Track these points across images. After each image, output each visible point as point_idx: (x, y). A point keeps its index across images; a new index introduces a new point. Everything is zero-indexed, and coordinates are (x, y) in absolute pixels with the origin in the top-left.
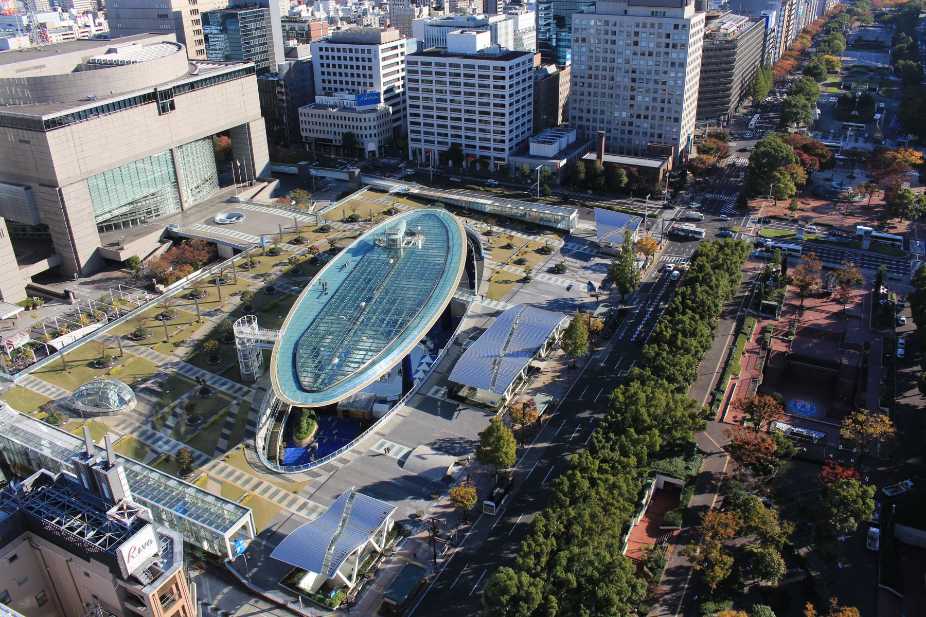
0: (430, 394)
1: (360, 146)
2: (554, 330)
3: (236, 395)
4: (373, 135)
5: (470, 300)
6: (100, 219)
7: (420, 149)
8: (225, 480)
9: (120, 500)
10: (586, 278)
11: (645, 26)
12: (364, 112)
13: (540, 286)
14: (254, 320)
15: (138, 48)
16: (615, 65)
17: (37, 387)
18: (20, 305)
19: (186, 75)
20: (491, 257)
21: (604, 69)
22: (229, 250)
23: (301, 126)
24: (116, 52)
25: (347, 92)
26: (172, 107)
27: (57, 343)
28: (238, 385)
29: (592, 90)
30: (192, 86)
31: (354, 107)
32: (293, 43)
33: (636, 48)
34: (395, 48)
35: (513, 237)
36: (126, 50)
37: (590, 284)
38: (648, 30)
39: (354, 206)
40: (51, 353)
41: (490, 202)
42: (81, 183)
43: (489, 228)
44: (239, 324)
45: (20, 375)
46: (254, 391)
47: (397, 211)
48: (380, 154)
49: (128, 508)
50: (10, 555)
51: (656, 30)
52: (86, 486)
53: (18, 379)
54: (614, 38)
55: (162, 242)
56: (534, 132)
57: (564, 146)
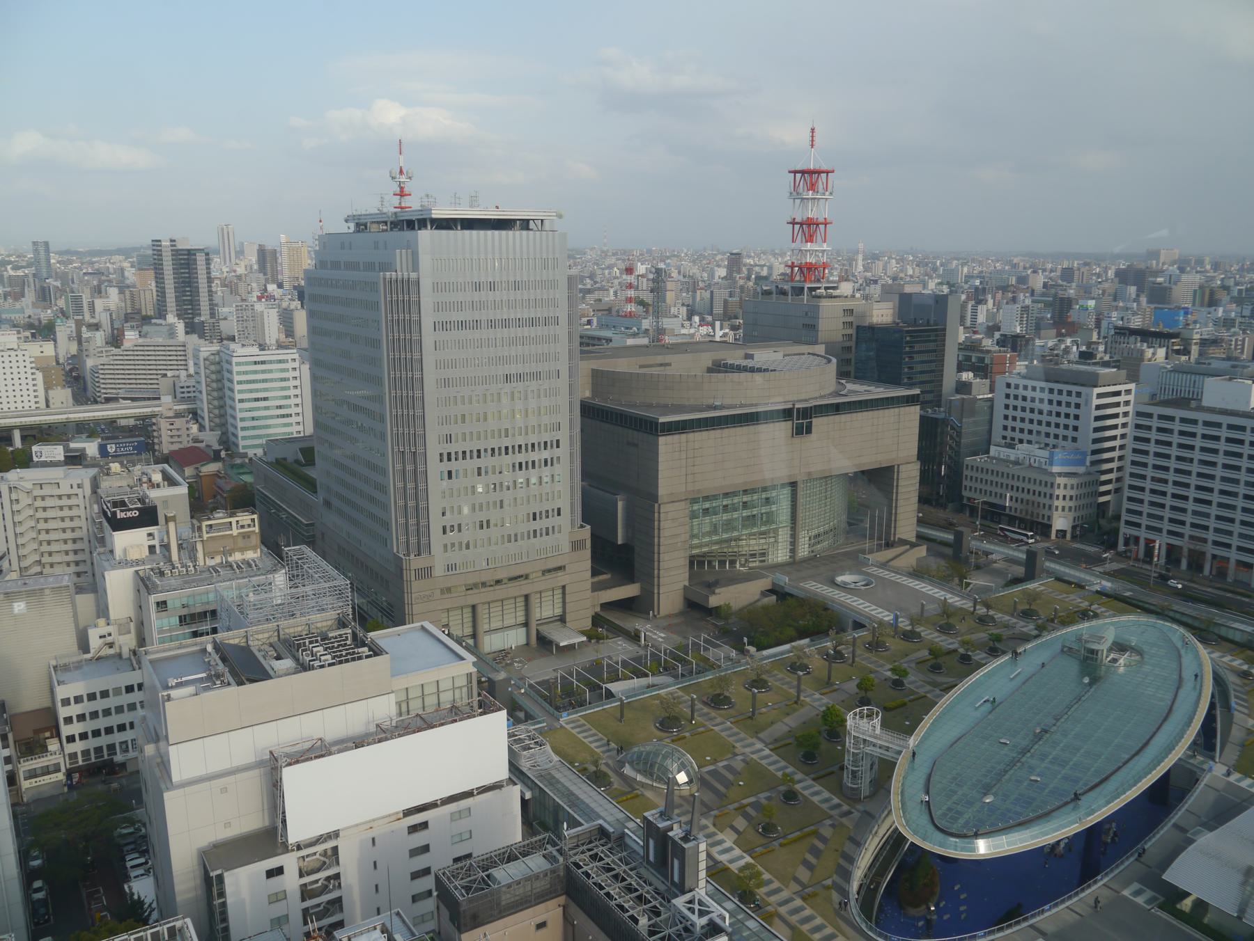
0: (1126, 893)
1: (1045, 521)
3: (833, 813)
4: (1067, 509)
5: (1206, 767)
6: (695, 552)
7: (1137, 539)
8: (798, 925)
9: (691, 891)
12: (1060, 474)
14: (877, 716)
15: (779, 356)
17: (585, 734)
18: (583, 633)
19: (830, 394)
20: (1246, 711)
22: (850, 624)
23: (965, 483)
24: (753, 359)
25: (1037, 446)
26: (809, 431)
27: (614, 687)
28: (836, 801)
30: (837, 409)
31: (1044, 467)
32: (967, 376)
34: (1118, 394)
36: (763, 356)
39: (1033, 597)
40: (607, 698)
42: (683, 502)
44: (855, 714)
45: (568, 715)
46: (856, 815)
47: (1096, 616)
48: (1074, 537)
49: (701, 903)
50: (539, 920)
52: (652, 858)
53: (565, 718)
55: (765, 593)
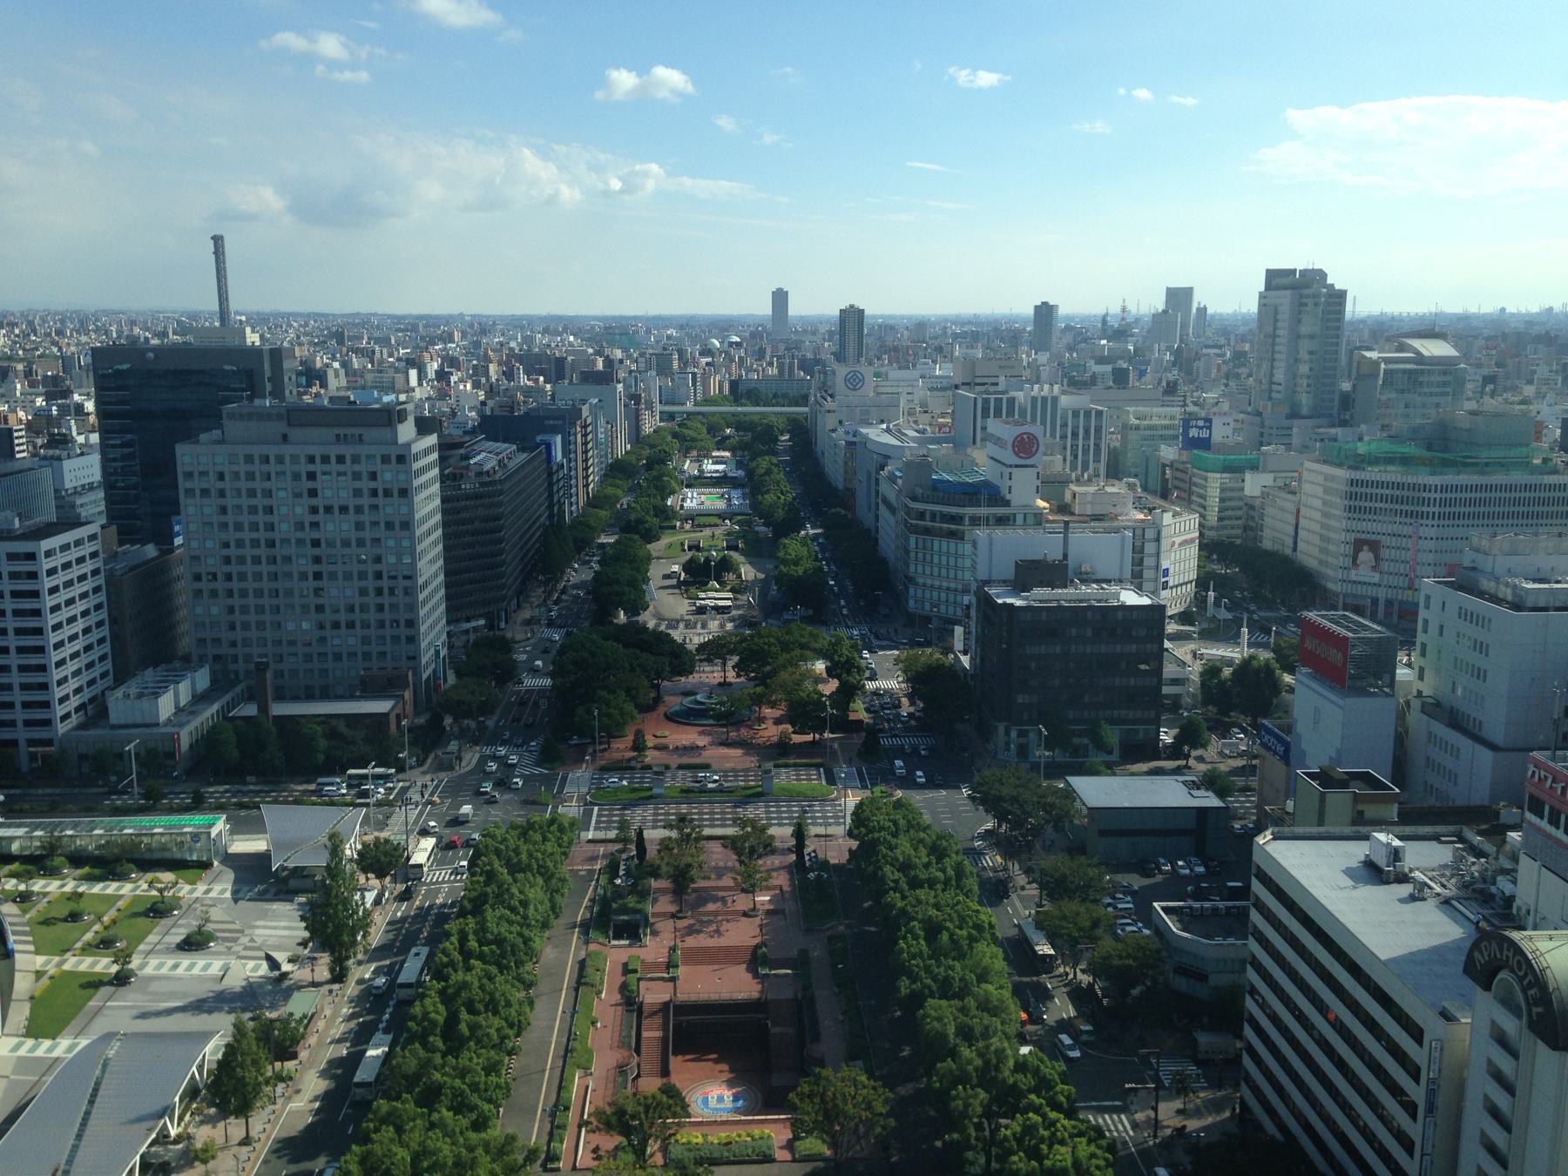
2: (194, 1068)
10: (259, 949)
11: (325, 459)
13: (154, 986)
16: (276, 535)
20: (31, 948)
21: (255, 543)
29: (235, 585)
33: (314, 501)
35: (81, 895)
37: (269, 958)
38: (334, 467)
41: (21, 832)
43: (22, 887)
51: (347, 467)
54: (267, 485)
56: (116, 680)
57: (184, 700)
